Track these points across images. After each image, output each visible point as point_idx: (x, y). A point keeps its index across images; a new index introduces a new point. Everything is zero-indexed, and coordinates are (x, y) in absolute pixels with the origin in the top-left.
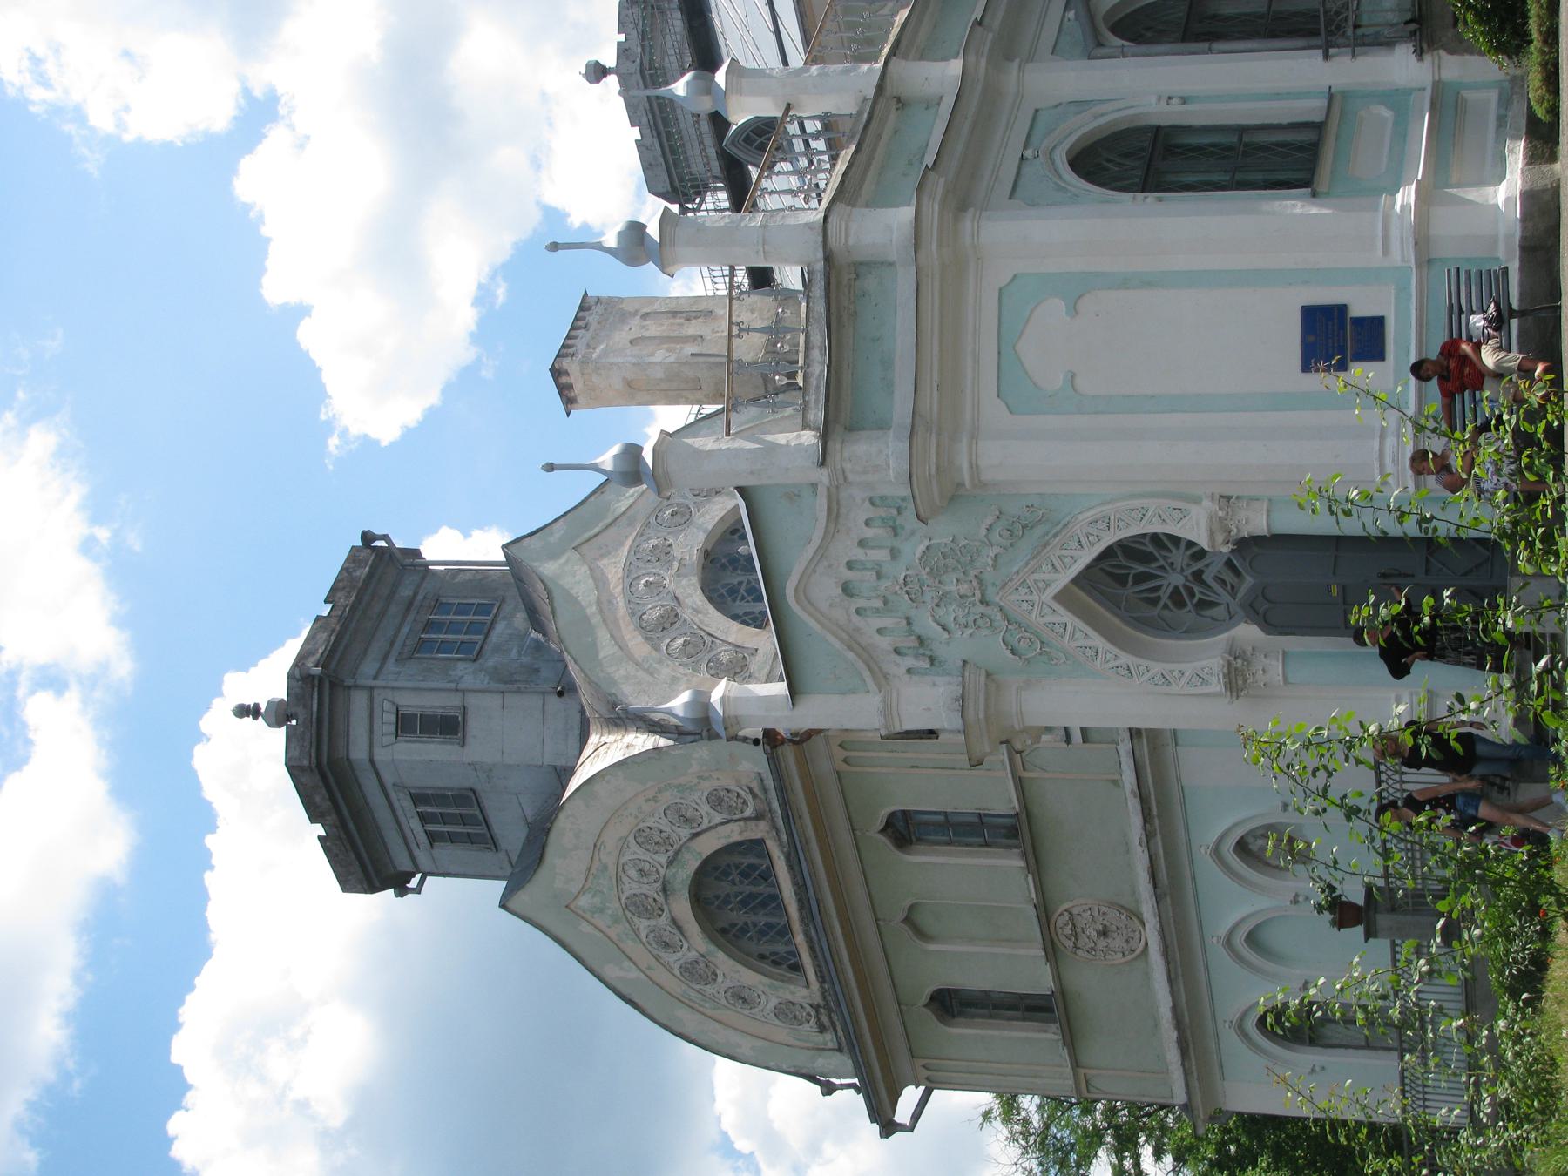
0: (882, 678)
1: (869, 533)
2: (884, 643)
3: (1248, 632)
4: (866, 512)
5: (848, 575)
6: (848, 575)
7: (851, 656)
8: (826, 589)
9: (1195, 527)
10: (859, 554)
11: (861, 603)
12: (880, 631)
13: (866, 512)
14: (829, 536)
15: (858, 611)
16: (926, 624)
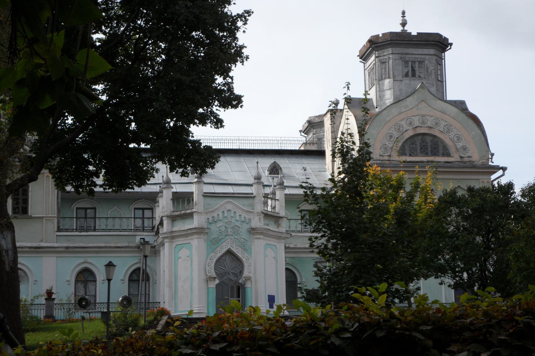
0: (207, 213)
1: (243, 217)
2: (215, 215)
3: (217, 281)
4: (247, 217)
5: (233, 211)
6: (233, 211)
7: (214, 208)
8: (229, 207)
9: (246, 274)
10: (238, 214)
11: (226, 213)
12: (218, 215)
13: (247, 217)
14: (243, 210)
15: (223, 212)
16: (219, 224)
